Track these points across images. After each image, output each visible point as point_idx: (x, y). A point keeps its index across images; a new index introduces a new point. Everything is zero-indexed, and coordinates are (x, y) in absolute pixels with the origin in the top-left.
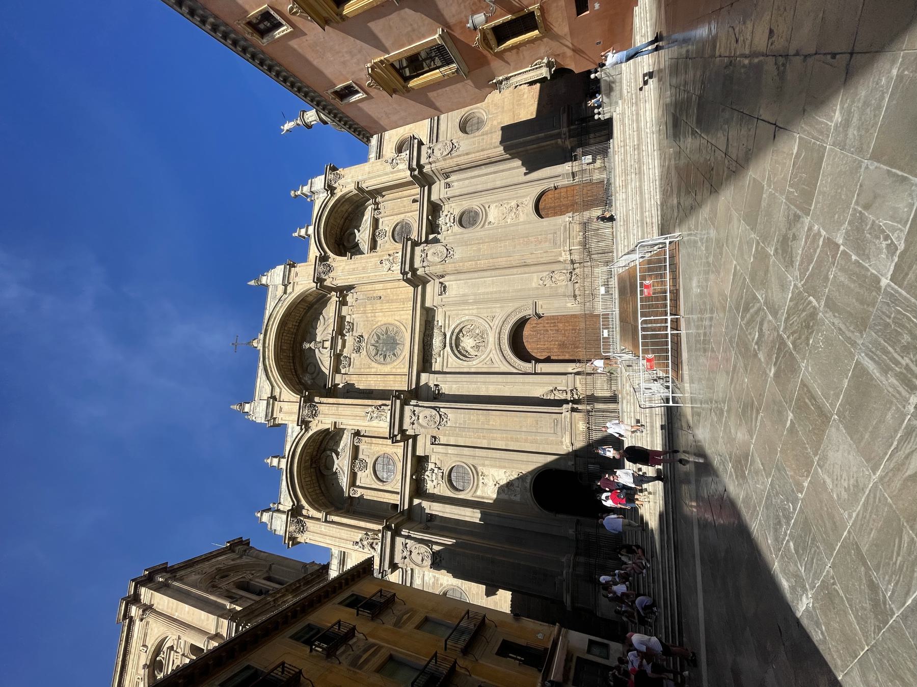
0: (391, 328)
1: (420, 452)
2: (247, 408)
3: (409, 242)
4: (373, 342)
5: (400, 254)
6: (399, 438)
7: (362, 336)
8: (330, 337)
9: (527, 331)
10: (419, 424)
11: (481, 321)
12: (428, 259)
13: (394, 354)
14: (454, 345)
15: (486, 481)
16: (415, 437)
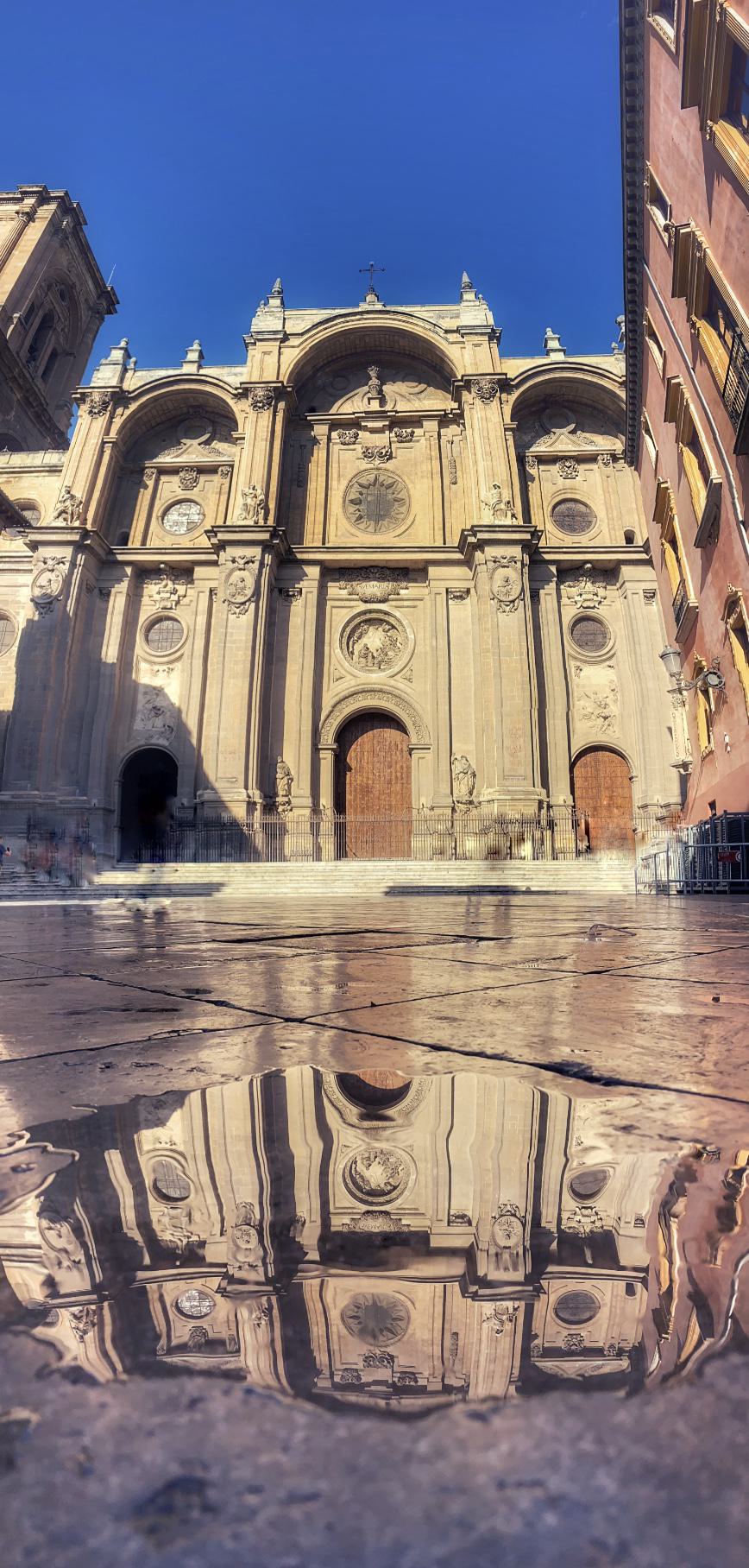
0: (403, 510)
1: (199, 572)
2: (275, 302)
3: (528, 536)
4: (381, 479)
5: (508, 522)
6: (214, 541)
7: (391, 458)
8: (388, 407)
9: (390, 734)
10: (232, 571)
11: (405, 660)
12: (503, 571)
13: (360, 517)
14: (368, 616)
15: (161, 674)
16: (215, 563)
